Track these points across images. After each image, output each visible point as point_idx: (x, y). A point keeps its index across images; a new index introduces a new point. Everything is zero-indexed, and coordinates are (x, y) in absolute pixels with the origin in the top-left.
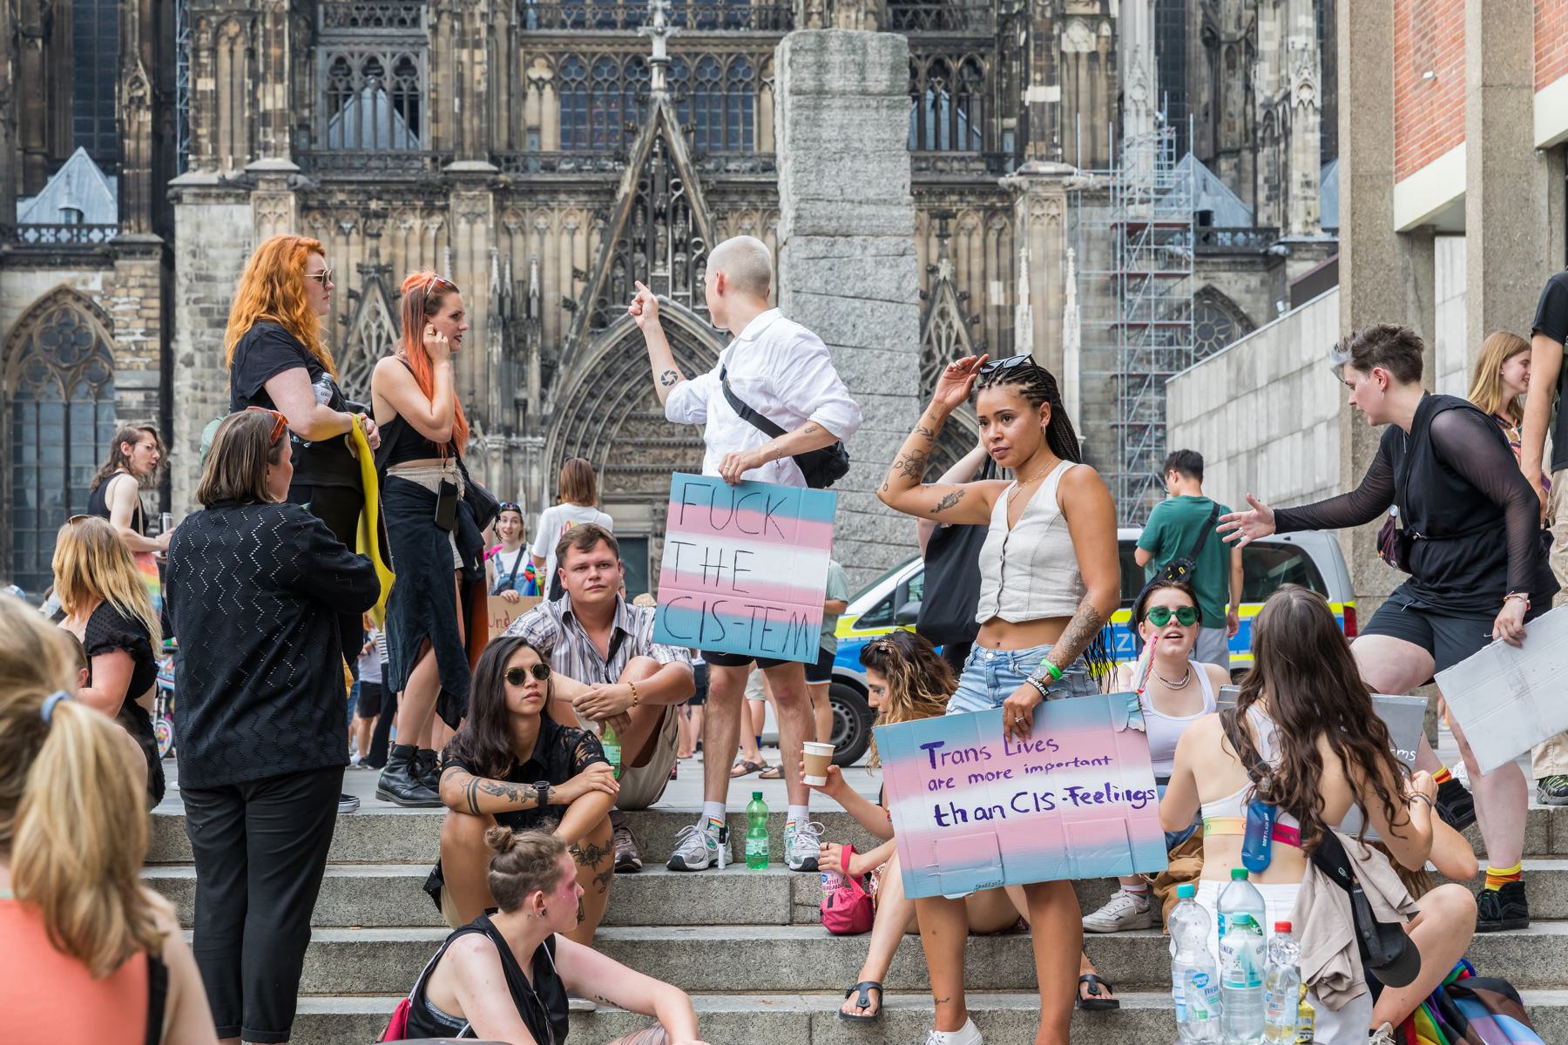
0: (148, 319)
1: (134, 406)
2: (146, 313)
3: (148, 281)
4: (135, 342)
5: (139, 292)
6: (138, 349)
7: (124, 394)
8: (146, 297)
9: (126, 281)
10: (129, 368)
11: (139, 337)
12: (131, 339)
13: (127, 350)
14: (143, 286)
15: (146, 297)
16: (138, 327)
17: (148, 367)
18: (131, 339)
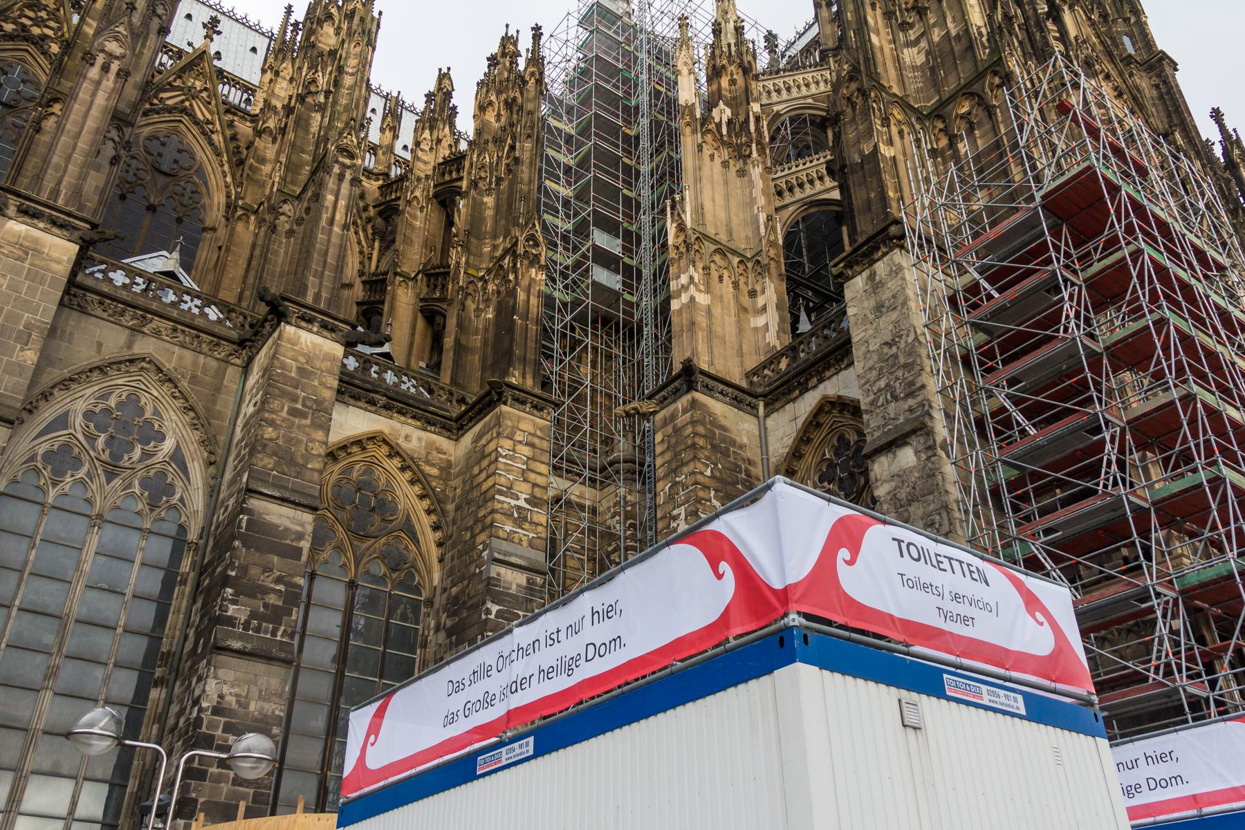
0: (535, 485)
1: (513, 590)
2: (532, 476)
3: (536, 441)
4: (519, 508)
5: (526, 451)
6: (521, 519)
7: (503, 570)
8: (533, 459)
9: (513, 433)
10: (509, 539)
11: (522, 503)
12: (513, 502)
13: (509, 515)
14: (530, 445)
15: (533, 459)
16: (523, 490)
17: (531, 545)
18: (513, 502)
